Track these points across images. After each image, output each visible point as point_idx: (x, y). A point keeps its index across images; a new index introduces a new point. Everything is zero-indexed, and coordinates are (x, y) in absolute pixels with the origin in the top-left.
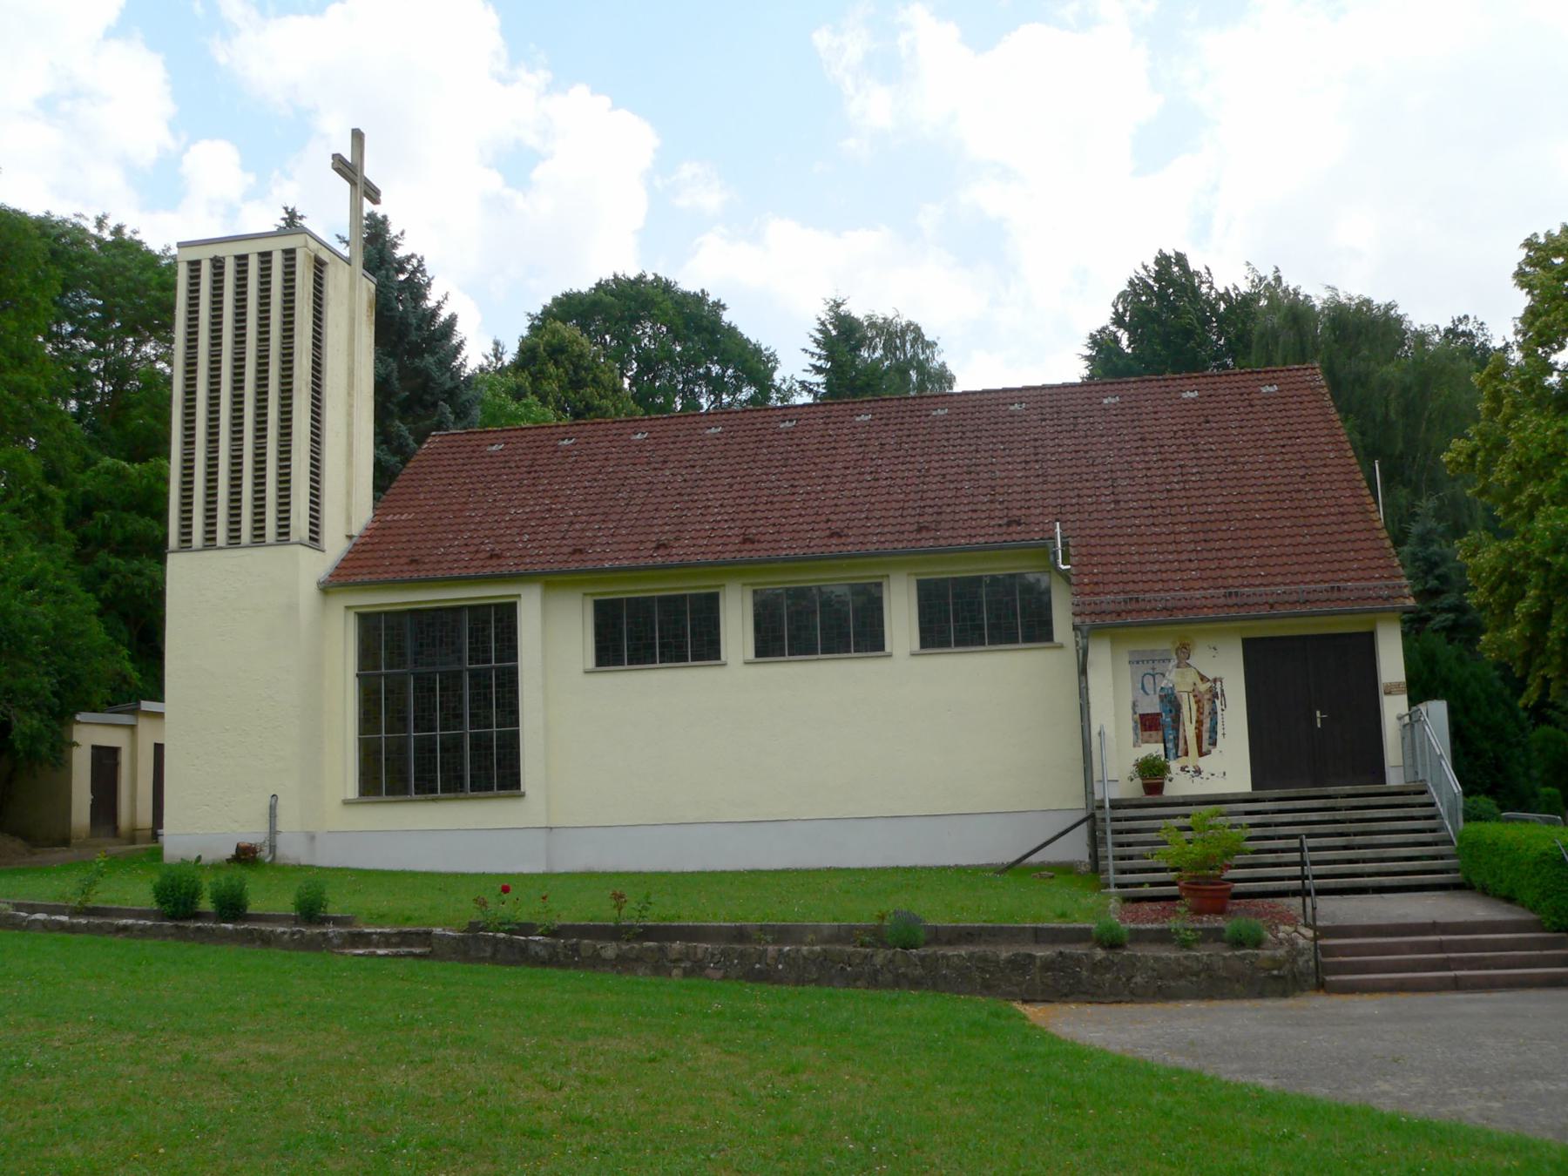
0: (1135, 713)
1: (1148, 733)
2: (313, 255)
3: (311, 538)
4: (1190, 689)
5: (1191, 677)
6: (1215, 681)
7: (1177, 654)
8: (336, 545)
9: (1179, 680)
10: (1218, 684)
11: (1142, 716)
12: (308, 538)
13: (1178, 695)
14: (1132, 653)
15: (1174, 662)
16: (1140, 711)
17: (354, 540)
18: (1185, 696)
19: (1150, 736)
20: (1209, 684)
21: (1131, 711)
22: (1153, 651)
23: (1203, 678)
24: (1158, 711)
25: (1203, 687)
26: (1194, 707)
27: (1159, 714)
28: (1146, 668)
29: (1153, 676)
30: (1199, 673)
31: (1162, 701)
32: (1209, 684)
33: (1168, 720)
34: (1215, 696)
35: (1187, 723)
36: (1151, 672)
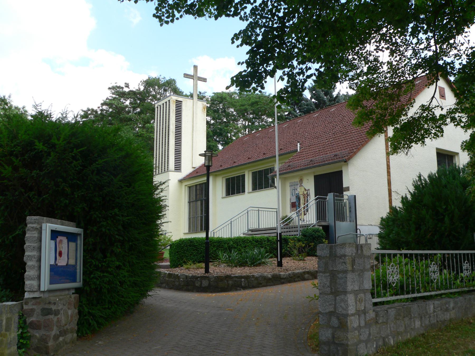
2: (175, 100)
4: (302, 193)
5: (303, 190)
6: (308, 190)
8: (187, 169)
9: (300, 191)
11: (292, 203)
14: (290, 183)
15: (299, 185)
16: (292, 202)
17: (196, 168)
18: (301, 195)
22: (294, 182)
23: (305, 190)
25: (305, 193)
27: (296, 202)
28: (293, 188)
32: (307, 191)
34: (308, 195)
35: (302, 204)
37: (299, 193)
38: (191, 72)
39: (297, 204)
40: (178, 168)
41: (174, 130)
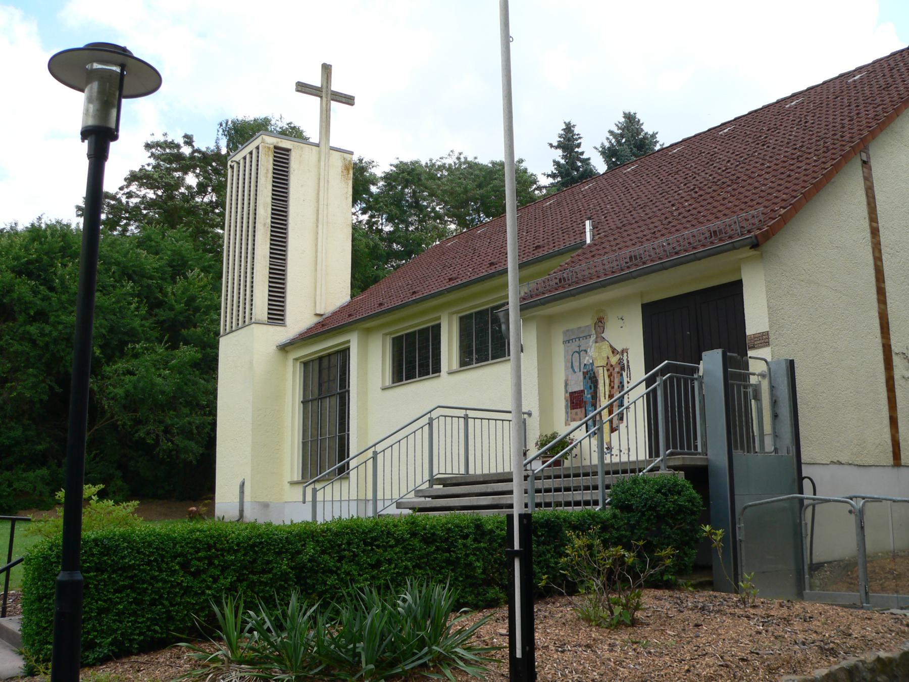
0: (566, 392)
1: (575, 410)
2: (272, 146)
3: (269, 318)
4: (604, 363)
5: (607, 351)
6: (623, 352)
7: (595, 329)
9: (597, 355)
10: (625, 354)
11: (572, 394)
12: (266, 319)
13: (595, 370)
14: (566, 333)
15: (593, 338)
16: (570, 391)
17: (324, 317)
18: (601, 370)
19: (576, 414)
20: (618, 356)
21: (563, 390)
23: (614, 351)
24: (582, 389)
25: (614, 360)
26: (607, 381)
27: (583, 391)
28: (574, 346)
29: (579, 353)
30: (611, 346)
31: (585, 378)
32: (618, 356)
33: (588, 396)
34: (623, 369)
35: (602, 399)
36: (577, 349)
37: (592, 364)
38: (316, 80)
39: (588, 396)
40: (277, 315)
41: (269, 220)
